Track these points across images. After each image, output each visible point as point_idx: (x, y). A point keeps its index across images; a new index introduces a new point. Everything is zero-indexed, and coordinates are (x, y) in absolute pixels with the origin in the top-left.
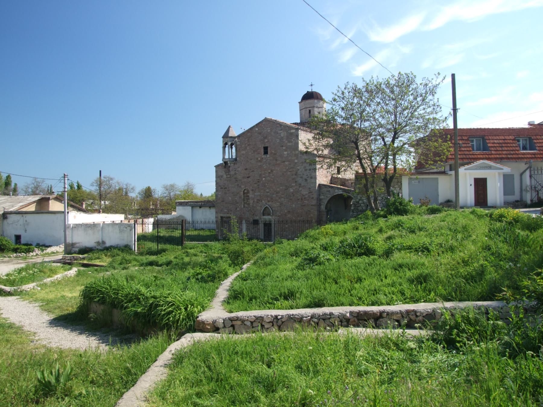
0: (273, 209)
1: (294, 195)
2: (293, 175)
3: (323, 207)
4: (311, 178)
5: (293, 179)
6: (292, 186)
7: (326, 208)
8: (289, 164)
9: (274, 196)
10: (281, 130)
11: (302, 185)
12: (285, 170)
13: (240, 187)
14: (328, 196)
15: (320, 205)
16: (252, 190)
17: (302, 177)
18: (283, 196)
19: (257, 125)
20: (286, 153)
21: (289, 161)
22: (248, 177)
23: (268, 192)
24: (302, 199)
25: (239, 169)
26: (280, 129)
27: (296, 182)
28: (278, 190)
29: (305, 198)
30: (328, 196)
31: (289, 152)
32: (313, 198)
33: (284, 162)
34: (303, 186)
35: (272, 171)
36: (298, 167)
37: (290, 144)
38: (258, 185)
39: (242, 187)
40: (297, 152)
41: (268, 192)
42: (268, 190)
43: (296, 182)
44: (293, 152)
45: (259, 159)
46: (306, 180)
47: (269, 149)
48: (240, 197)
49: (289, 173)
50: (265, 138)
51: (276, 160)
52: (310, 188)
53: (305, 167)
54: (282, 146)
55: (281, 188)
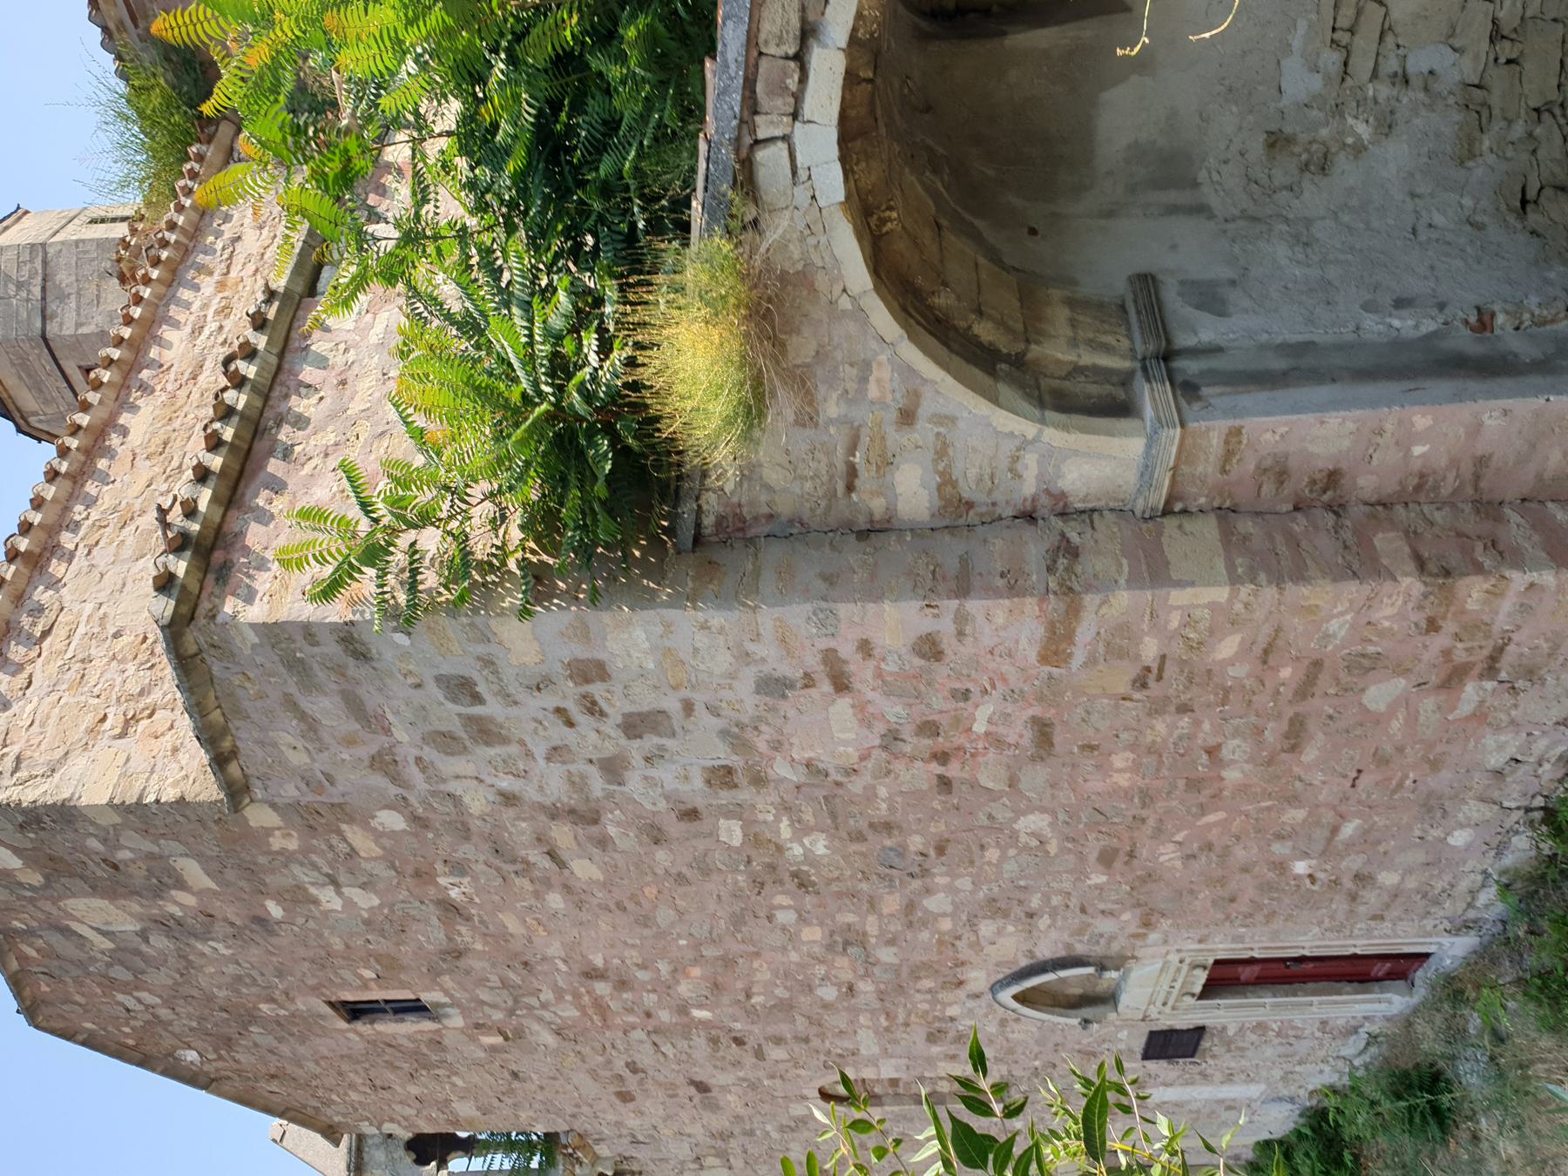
0: (1045, 952)
3: (1098, 462)
4: (590, 671)
6: (754, 839)
7: (1115, 407)
8: (459, 868)
9: (887, 955)
10: (66, 932)
12: (555, 900)
14: (883, 384)
15: (1058, 535)
17: (613, 768)
19: (144, 1062)
20: (329, 899)
21: (423, 875)
22: (702, 1088)
24: (942, 757)
26: (55, 939)
28: (813, 934)
30: (883, 384)
31: (302, 874)
33: (450, 910)
35: (592, 974)
37: (192, 870)
43: (692, 814)
47: (350, 997)
49: (584, 869)
50: (252, 1017)
51: (459, 954)
53: (446, 742)
54: (262, 921)
55: (785, 917)
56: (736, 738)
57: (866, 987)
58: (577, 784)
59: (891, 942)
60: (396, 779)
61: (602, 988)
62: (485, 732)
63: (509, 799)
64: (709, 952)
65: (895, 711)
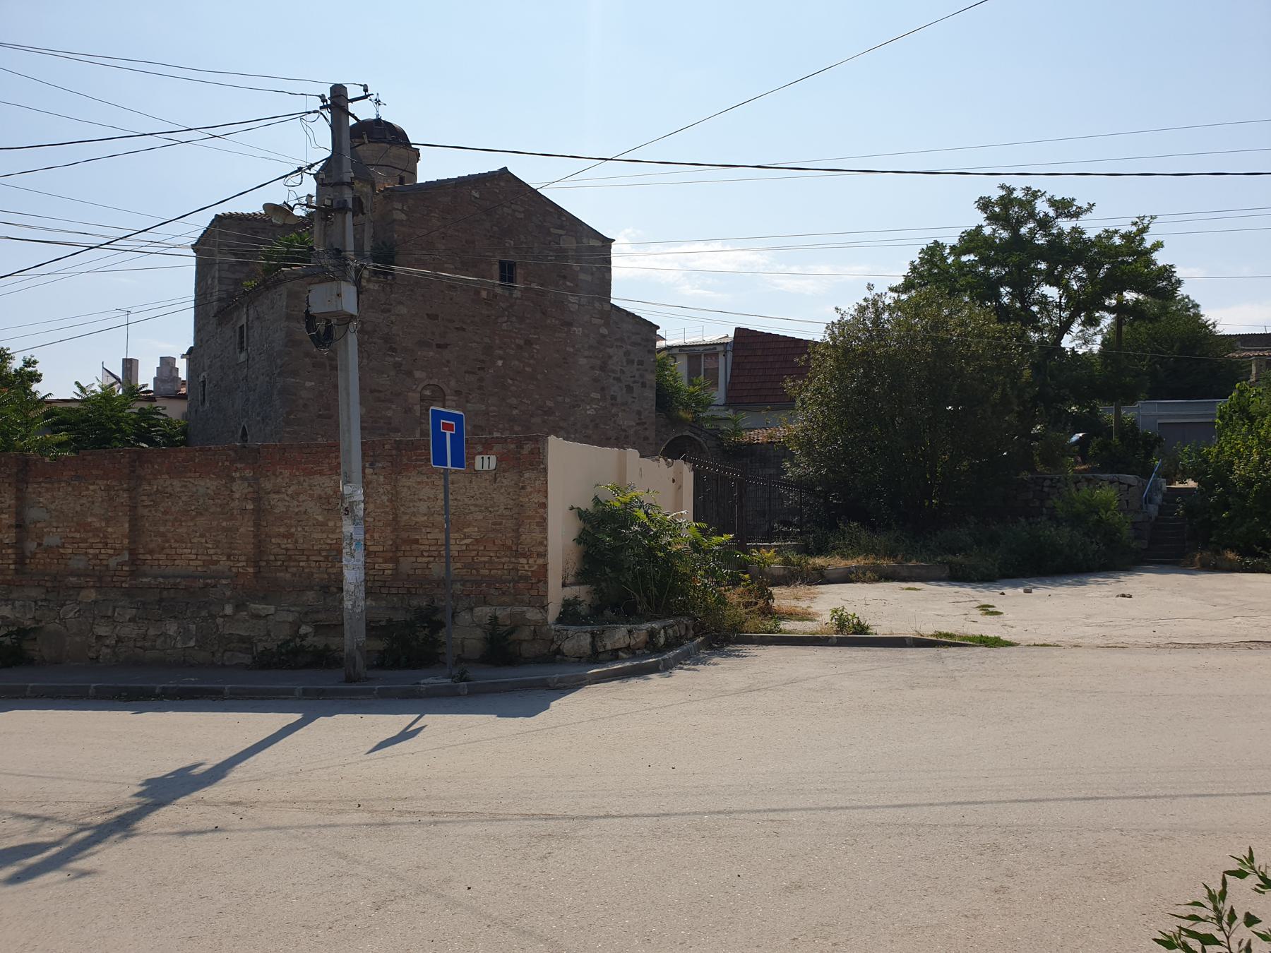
1: (596, 426)
2: (593, 368)
5: (596, 380)
9: (536, 420)
10: (561, 227)
11: (619, 400)
13: (409, 374)
16: (458, 393)
17: (618, 380)
18: (562, 424)
23: (513, 407)
24: (617, 439)
25: (403, 310)
27: (603, 389)
28: (549, 404)
29: (626, 437)
32: (646, 439)
34: (623, 404)
35: (529, 343)
36: (609, 350)
38: (481, 380)
39: (418, 374)
40: (607, 308)
41: (513, 407)
42: (514, 401)
43: (603, 389)
44: (597, 304)
45: (484, 294)
46: (629, 389)
48: (408, 410)
52: (639, 413)
53: (627, 353)
54: (565, 277)
55: (560, 399)
56: (625, 404)
57: (515, 412)
58: (613, 371)
59: (544, 422)
60: (617, 340)
61: (521, 342)
62: (630, 362)
63: (610, 357)
64: (539, 377)
65: (632, 432)
